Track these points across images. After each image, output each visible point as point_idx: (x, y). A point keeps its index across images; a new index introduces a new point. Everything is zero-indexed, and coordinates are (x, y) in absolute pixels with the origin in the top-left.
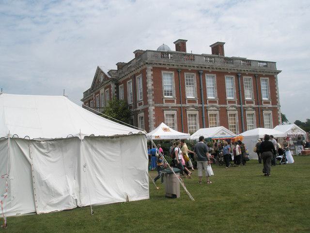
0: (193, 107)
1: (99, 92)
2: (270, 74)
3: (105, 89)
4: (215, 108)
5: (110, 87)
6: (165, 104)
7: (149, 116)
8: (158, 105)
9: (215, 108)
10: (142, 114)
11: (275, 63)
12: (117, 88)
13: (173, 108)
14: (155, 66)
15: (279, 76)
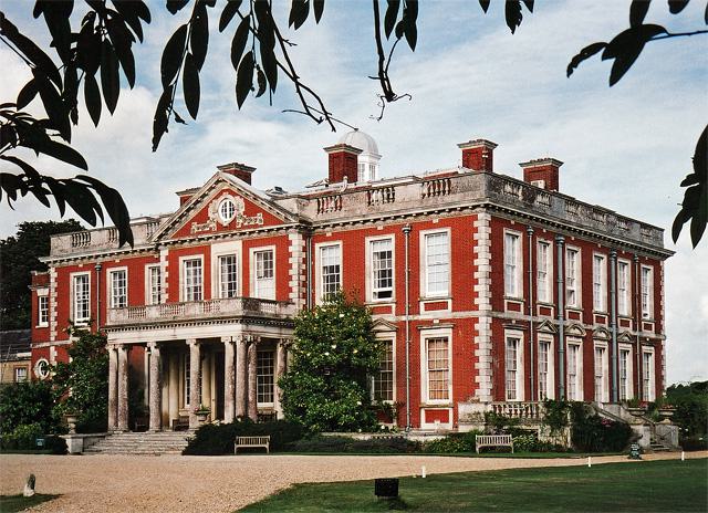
0: (547, 325)
1: (206, 250)
2: (657, 258)
3: (246, 246)
4: (577, 331)
5: (284, 243)
6: (507, 314)
7: (490, 333)
8: (495, 314)
9: (577, 331)
10: (447, 332)
11: (663, 230)
12: (308, 250)
13: (520, 325)
14: (497, 214)
15: (667, 264)
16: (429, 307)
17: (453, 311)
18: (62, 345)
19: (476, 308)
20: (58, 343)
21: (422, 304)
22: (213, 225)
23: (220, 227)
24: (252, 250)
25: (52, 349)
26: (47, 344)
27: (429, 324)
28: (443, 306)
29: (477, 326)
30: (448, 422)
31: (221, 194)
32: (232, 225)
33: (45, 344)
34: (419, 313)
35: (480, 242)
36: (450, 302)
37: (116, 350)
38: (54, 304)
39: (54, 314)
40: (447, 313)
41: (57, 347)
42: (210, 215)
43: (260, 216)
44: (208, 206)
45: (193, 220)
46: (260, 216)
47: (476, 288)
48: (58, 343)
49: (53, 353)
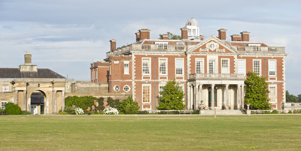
1: (205, 57)
3: (220, 58)
10: (276, 86)
16: (271, 79)
17: (277, 80)
18: (138, 81)
19: (283, 80)
20: (136, 80)
21: (269, 78)
22: (208, 50)
23: (210, 51)
24: (222, 59)
25: (133, 82)
26: (131, 80)
27: (271, 83)
28: (275, 79)
29: (283, 85)
30: (276, 107)
31: (211, 41)
32: (215, 51)
33: (131, 80)
34: (268, 80)
35: (284, 64)
36: (276, 78)
37: (199, 86)
38: (134, 67)
39: (134, 71)
40: (276, 81)
41: (135, 82)
42: (206, 47)
43: (224, 49)
44: (206, 44)
45: (200, 47)
46: (224, 49)
47: (283, 75)
48: (136, 80)
49: (134, 84)
